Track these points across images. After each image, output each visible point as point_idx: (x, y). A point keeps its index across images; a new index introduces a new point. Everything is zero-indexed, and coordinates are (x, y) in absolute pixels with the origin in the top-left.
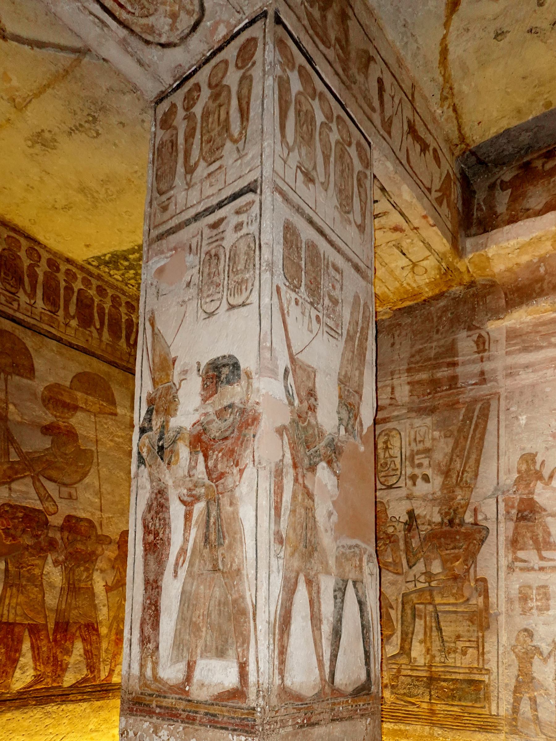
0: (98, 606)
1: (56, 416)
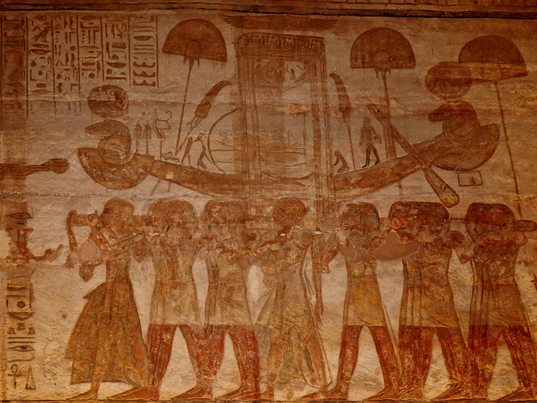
0: (526, 306)
1: (445, 98)
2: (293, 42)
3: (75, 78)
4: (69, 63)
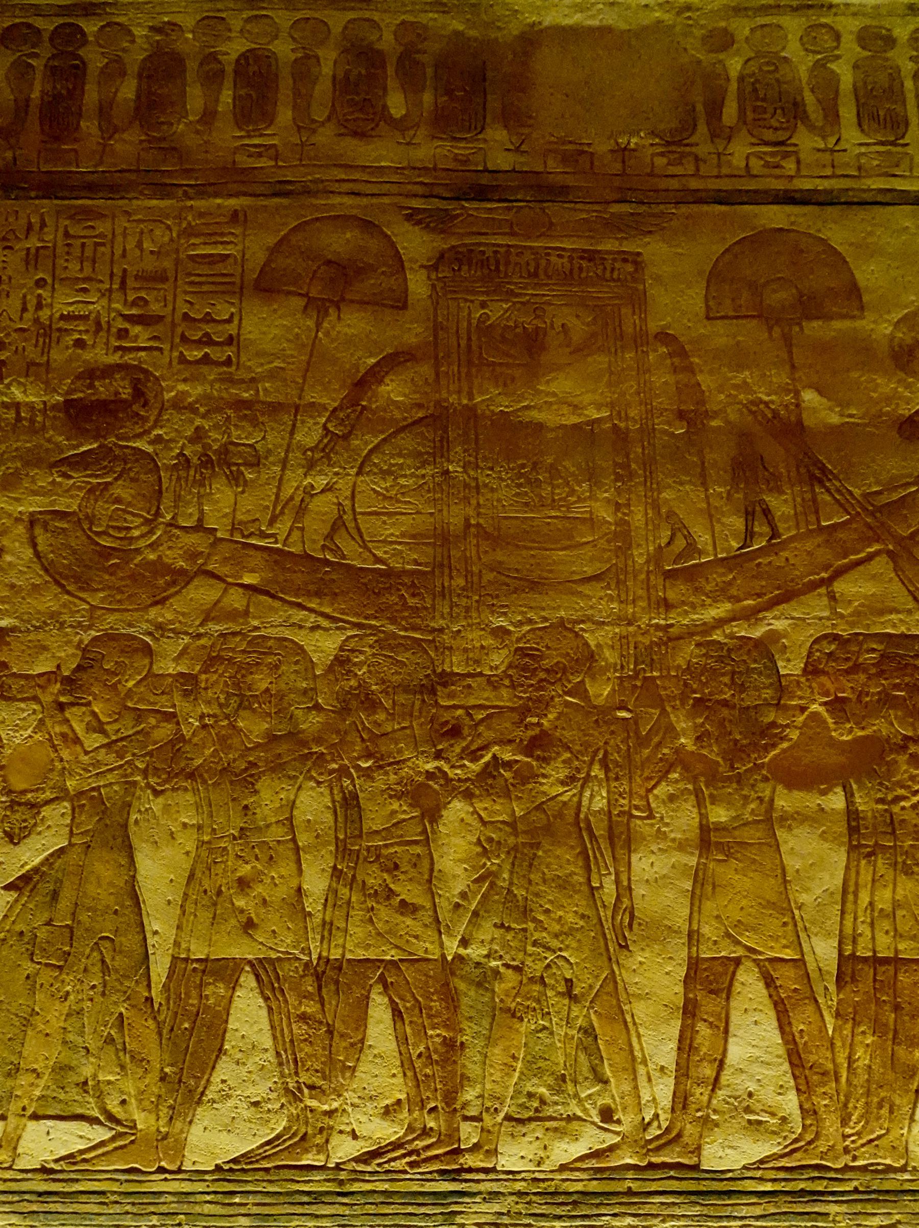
3: (39, 349)
4: (28, 316)
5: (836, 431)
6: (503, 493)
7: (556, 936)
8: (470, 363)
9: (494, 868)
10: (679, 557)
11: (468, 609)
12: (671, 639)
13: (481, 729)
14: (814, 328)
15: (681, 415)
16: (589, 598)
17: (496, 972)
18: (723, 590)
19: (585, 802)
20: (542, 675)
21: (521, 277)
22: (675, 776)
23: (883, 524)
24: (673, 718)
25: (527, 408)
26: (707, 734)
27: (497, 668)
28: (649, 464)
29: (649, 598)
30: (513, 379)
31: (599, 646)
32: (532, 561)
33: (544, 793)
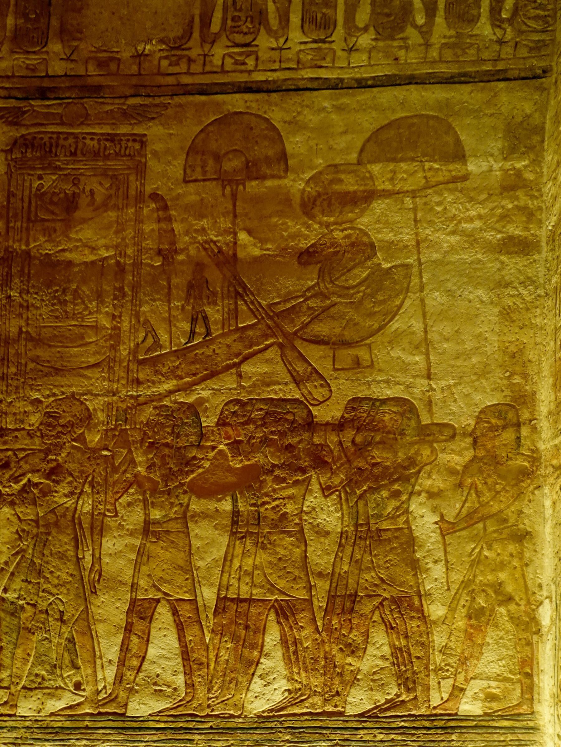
2: (96, 146)
5: (257, 260)
6: (44, 310)
7: (56, 586)
8: (29, 219)
9: (25, 547)
10: (149, 350)
11: (17, 388)
12: (140, 404)
13: (22, 463)
14: (253, 187)
15: (159, 252)
16: (90, 378)
17: (22, 607)
18: (172, 371)
19: (79, 508)
20: (60, 429)
21: (65, 156)
22: (132, 491)
23: (277, 326)
24: (135, 455)
25: (63, 250)
26: (154, 465)
27: (33, 425)
28: (135, 288)
29: (128, 379)
30: (55, 231)
31: (95, 409)
32: (58, 355)
33: (56, 502)
